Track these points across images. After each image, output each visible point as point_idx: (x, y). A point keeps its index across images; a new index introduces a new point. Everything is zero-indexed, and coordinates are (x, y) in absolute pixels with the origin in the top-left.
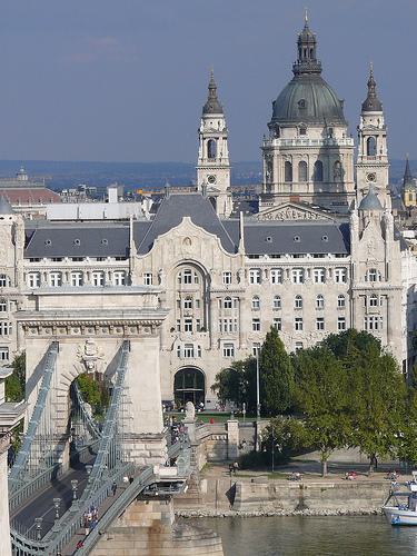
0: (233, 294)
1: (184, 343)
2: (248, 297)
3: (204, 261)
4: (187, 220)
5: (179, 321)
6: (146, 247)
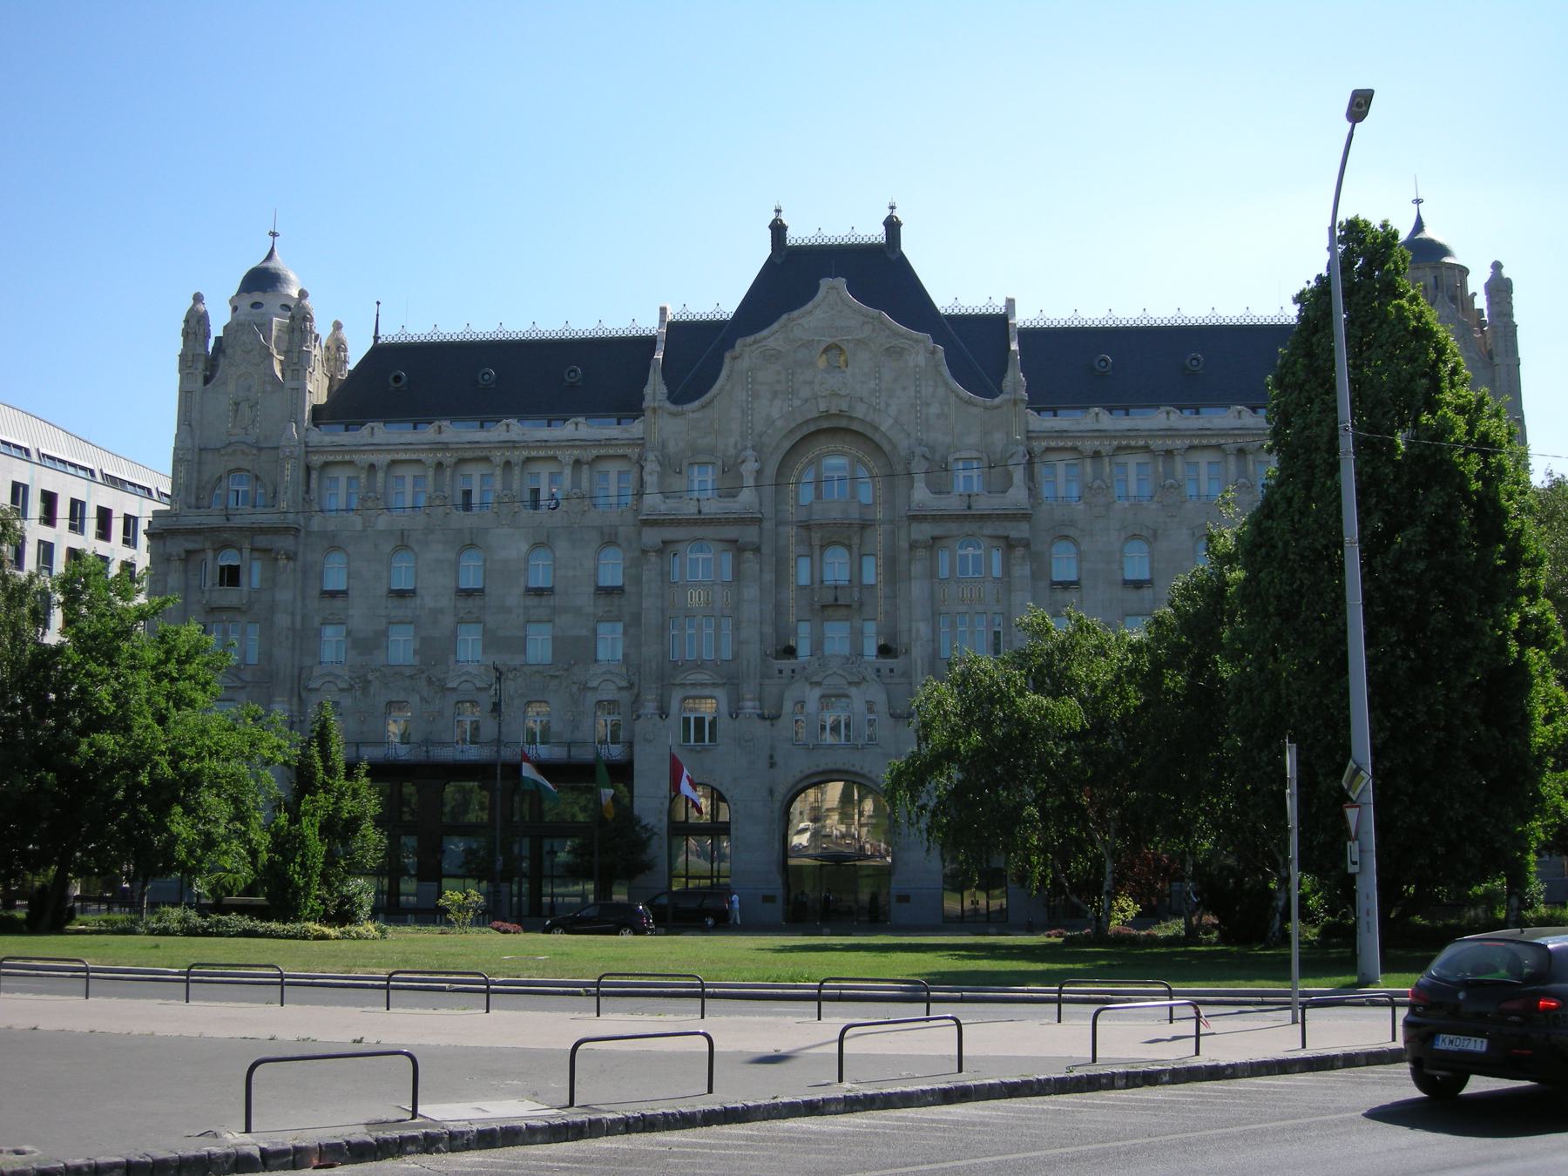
0: (989, 529)
1: (817, 692)
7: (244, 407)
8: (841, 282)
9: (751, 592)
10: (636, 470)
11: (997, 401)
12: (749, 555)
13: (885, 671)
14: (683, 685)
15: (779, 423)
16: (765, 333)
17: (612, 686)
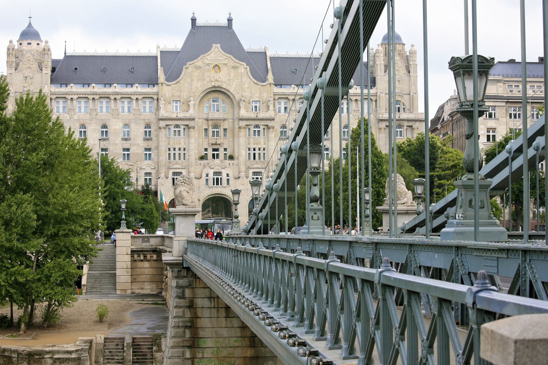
0: (263, 123)
1: (212, 171)
2: (277, 125)
3: (232, 89)
4: (216, 48)
5: (206, 150)
6: (173, 76)
7: (28, 78)
8: (219, 45)
9: (192, 141)
10: (156, 101)
11: (264, 84)
12: (192, 129)
13: (231, 164)
15: (200, 89)
16: (196, 61)
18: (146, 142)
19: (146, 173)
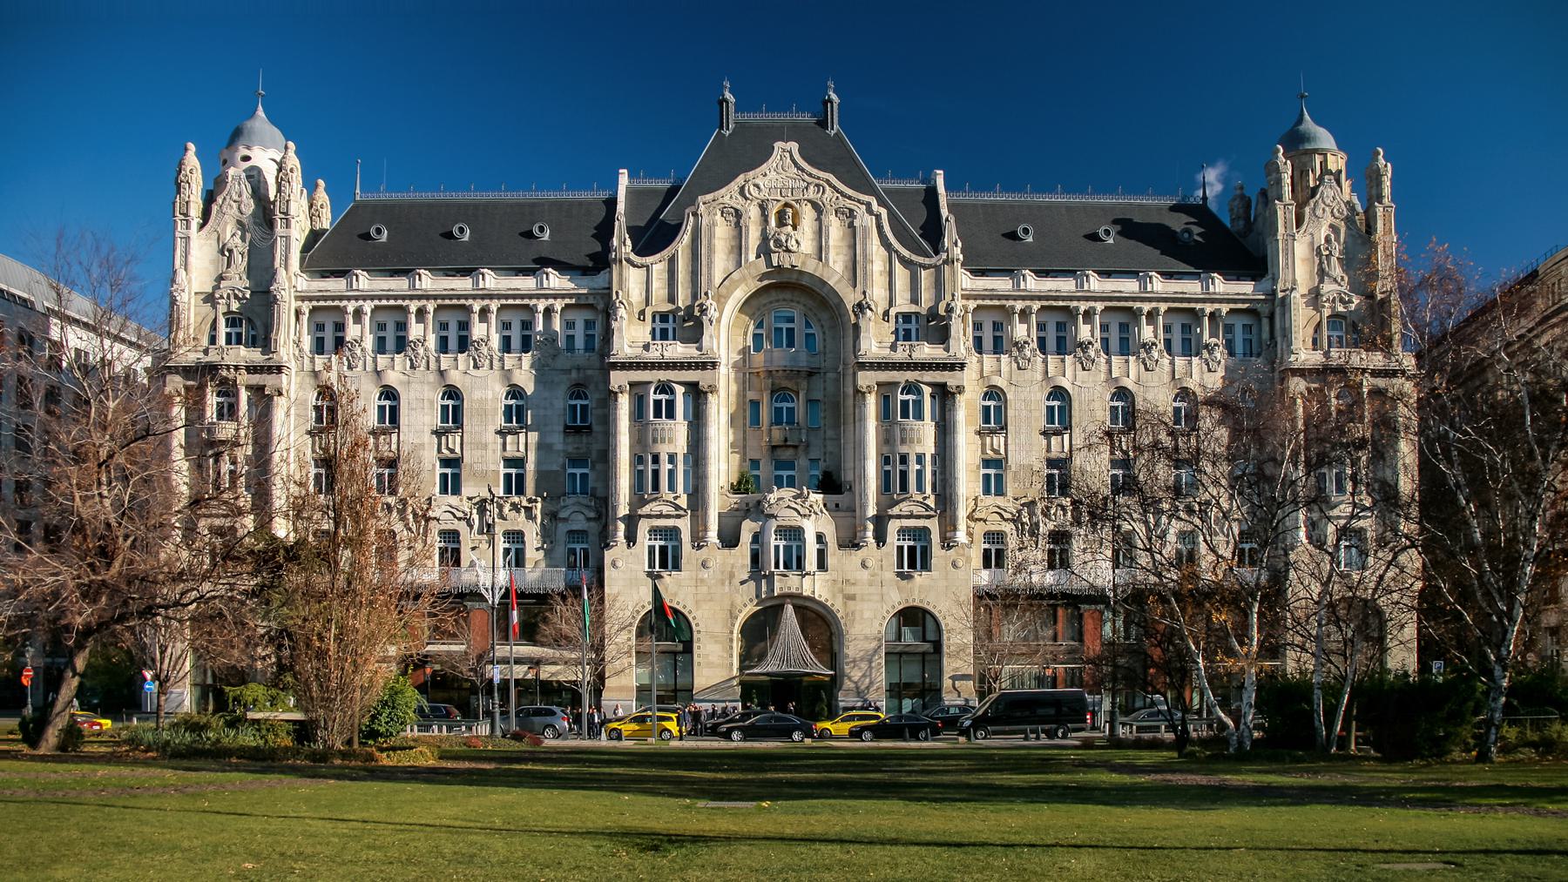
0: (930, 376)
4: (785, 151)
14: (649, 516)
17: (581, 517)
18: (570, 439)
19: (571, 532)
